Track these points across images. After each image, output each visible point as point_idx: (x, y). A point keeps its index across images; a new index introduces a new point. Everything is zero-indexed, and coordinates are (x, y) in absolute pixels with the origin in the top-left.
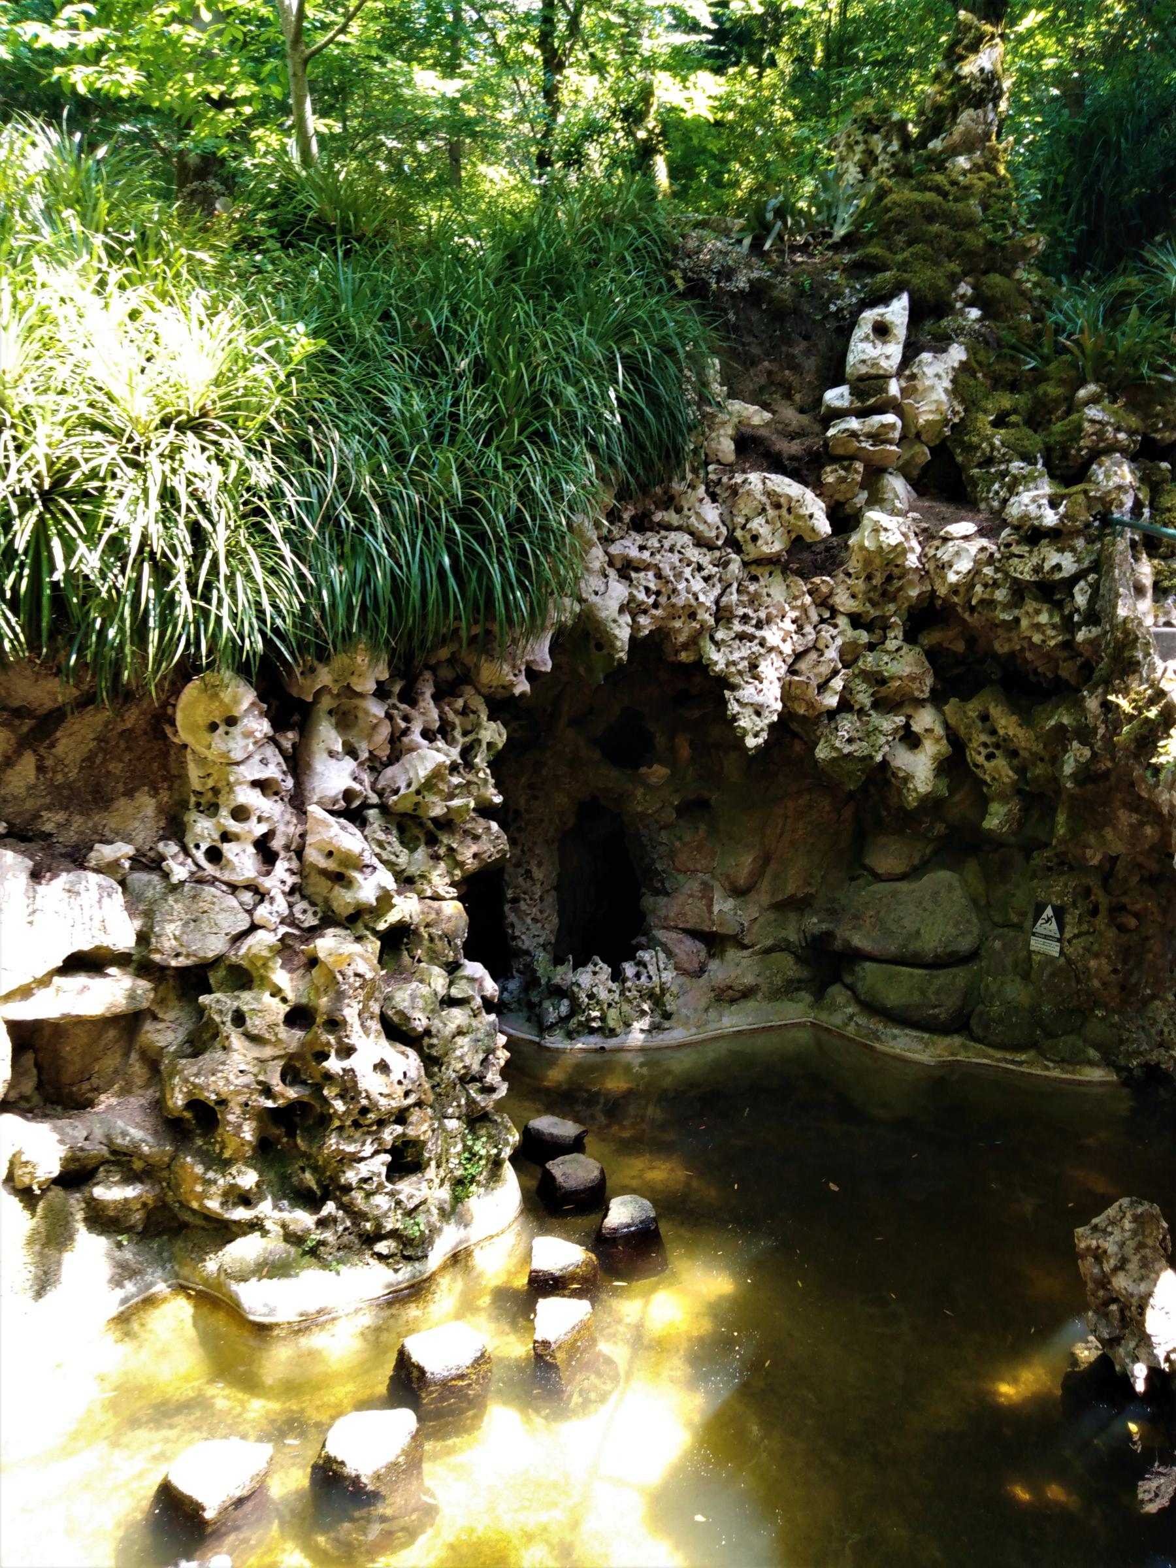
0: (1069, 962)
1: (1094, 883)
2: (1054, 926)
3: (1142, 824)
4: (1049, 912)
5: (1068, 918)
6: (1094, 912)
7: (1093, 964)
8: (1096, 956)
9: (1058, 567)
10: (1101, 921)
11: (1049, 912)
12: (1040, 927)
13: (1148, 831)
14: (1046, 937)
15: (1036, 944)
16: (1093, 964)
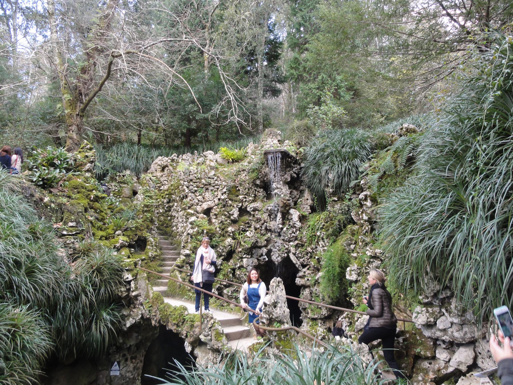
0: (122, 375)
1: (126, 353)
2: (117, 367)
3: (138, 336)
4: (116, 363)
5: (121, 364)
6: (126, 360)
7: (127, 374)
8: (128, 372)
9: (128, 278)
10: (129, 362)
11: (116, 363)
12: (113, 368)
13: (140, 337)
14: (115, 370)
15: (112, 373)
16: (127, 374)
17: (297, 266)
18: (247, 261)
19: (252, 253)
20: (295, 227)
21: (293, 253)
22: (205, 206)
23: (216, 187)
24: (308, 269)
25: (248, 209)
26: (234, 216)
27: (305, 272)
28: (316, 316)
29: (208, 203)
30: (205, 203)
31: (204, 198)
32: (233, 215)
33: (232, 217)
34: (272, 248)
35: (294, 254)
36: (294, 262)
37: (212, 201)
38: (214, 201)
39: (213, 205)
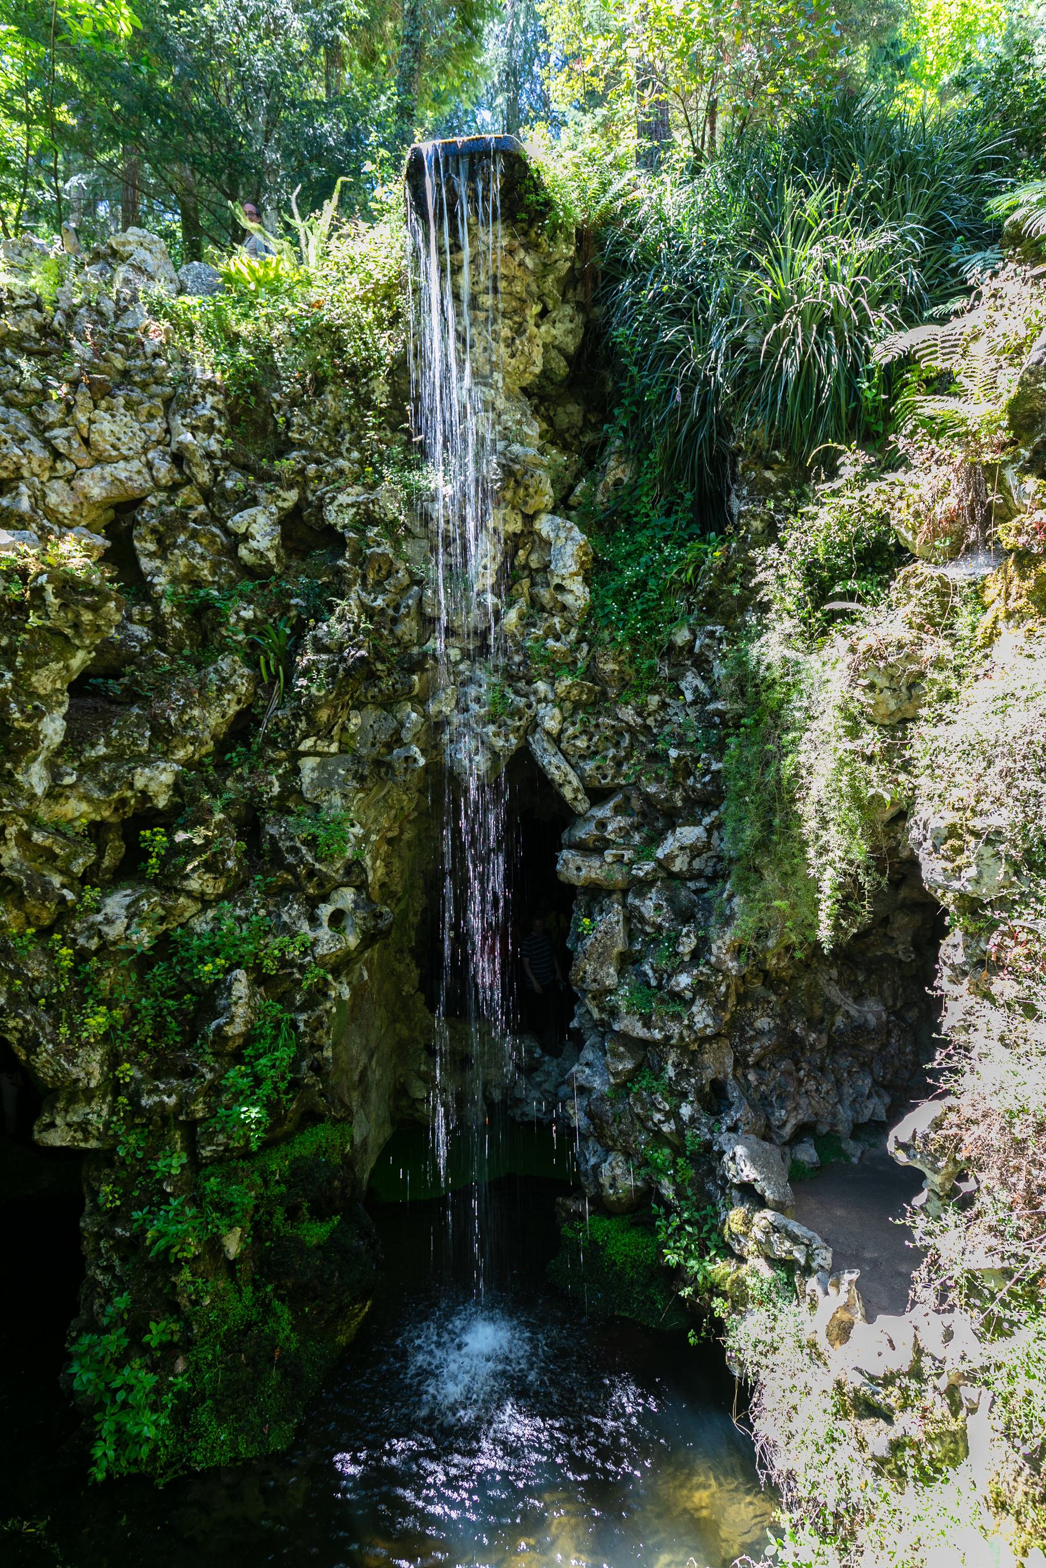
17: (568, 793)
18: (321, 767)
19: (344, 729)
20: (564, 608)
21: (548, 733)
22: (95, 485)
23: (155, 389)
24: (617, 810)
25: (331, 516)
26: (253, 544)
27: (602, 825)
28: (658, 1035)
29: (109, 469)
30: (98, 470)
31: (86, 441)
32: (246, 537)
33: (243, 552)
34: (446, 710)
35: (556, 740)
36: (557, 776)
37: (136, 465)
38: (150, 466)
39: (142, 481)
